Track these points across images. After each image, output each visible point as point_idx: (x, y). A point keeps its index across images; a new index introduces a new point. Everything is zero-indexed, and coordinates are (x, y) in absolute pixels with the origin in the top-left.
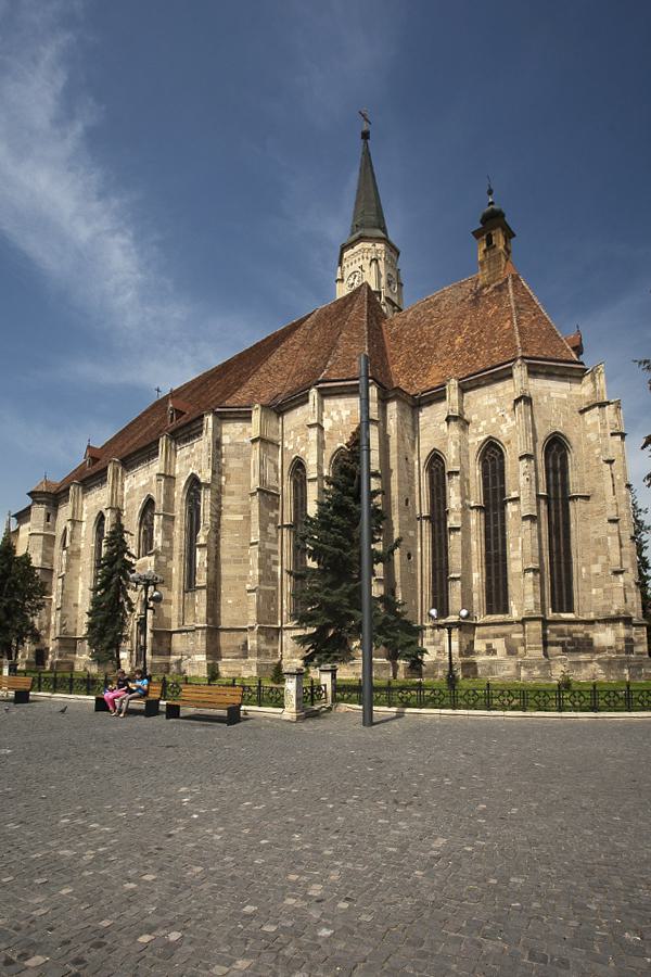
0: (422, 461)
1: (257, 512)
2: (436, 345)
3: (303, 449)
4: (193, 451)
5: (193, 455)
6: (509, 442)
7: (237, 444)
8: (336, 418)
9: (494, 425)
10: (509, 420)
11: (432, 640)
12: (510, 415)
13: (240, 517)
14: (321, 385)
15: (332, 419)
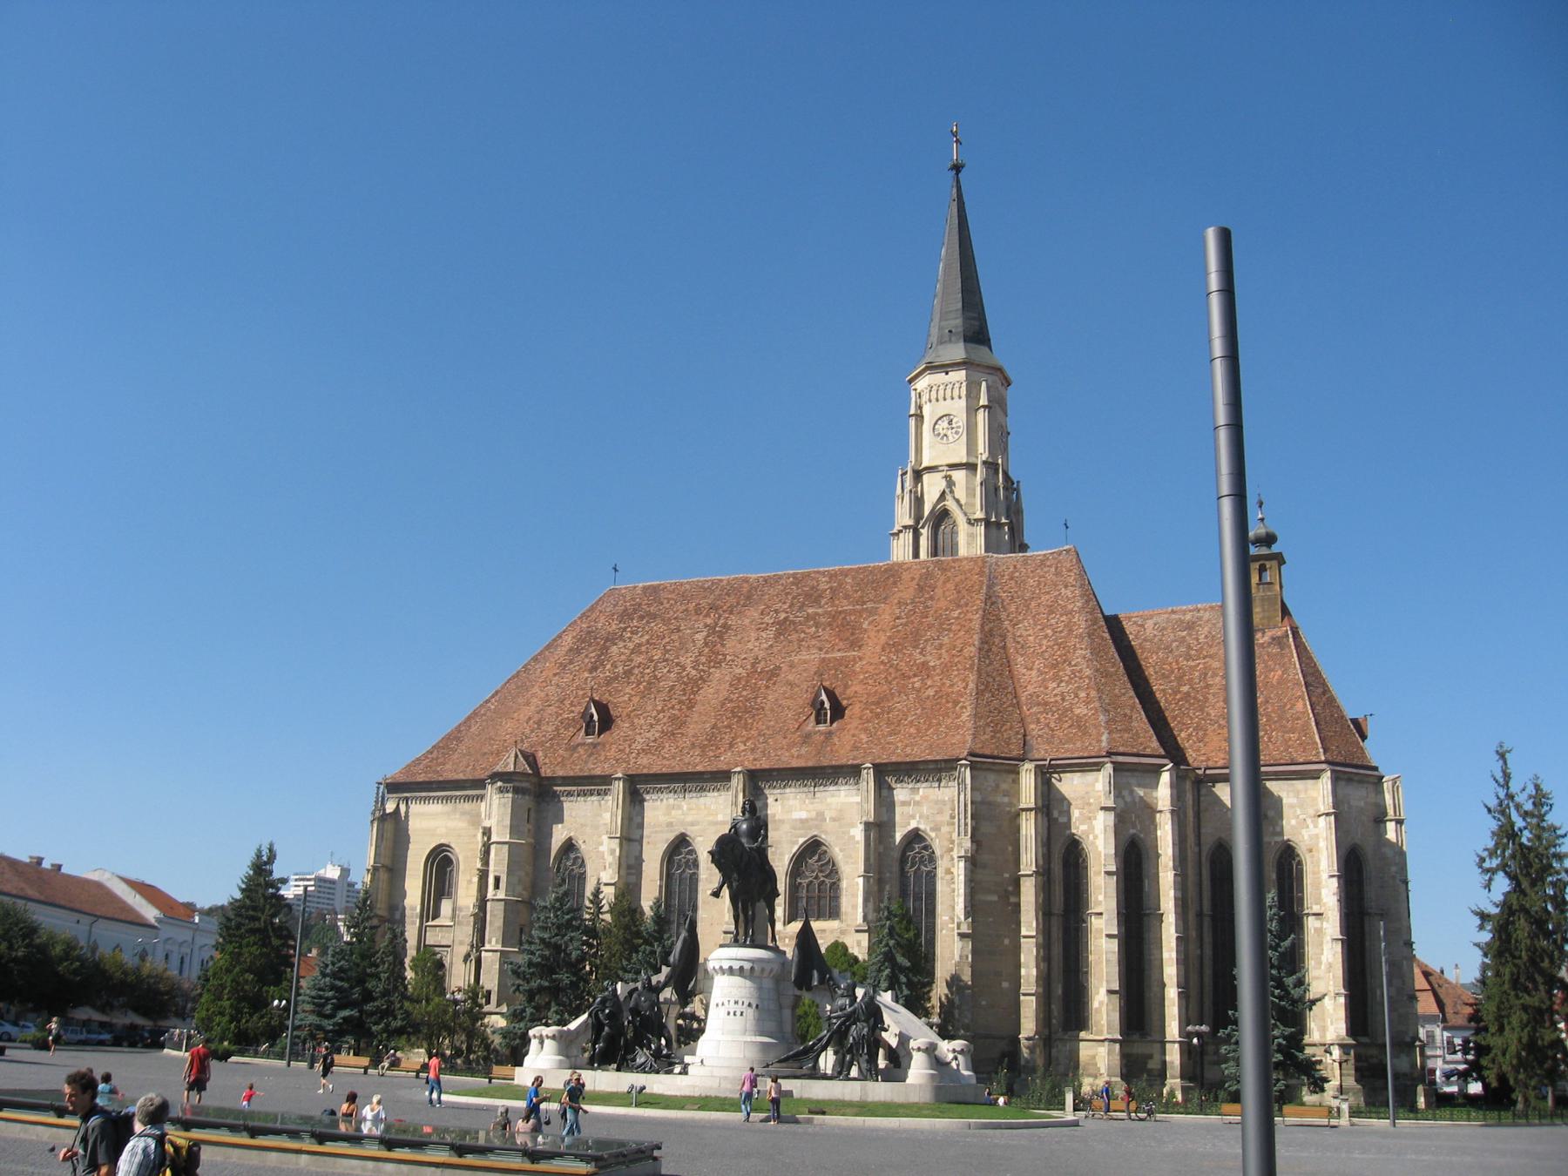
0: (1206, 849)
1: (1033, 899)
2: (1206, 699)
3: (1083, 827)
4: (917, 798)
5: (917, 803)
6: (1311, 851)
7: (990, 804)
8: (1128, 799)
9: (1292, 827)
10: (1311, 826)
11: (1215, 1058)
12: (1312, 822)
13: (995, 898)
14: (1115, 758)
15: (1123, 798)
